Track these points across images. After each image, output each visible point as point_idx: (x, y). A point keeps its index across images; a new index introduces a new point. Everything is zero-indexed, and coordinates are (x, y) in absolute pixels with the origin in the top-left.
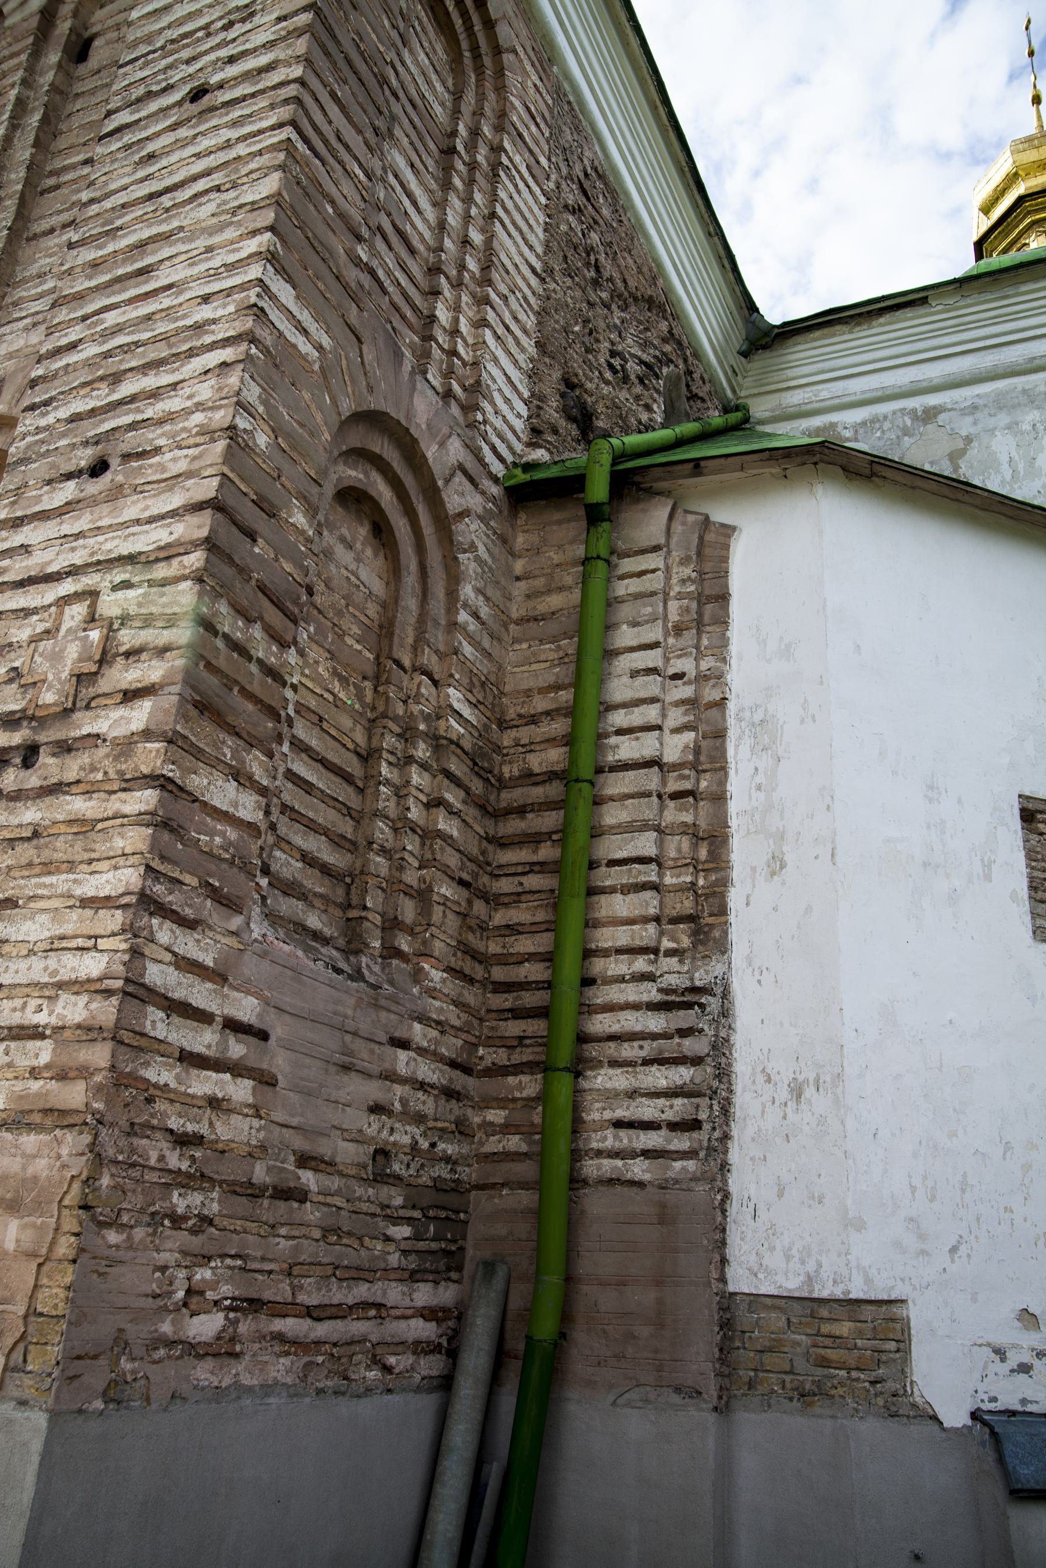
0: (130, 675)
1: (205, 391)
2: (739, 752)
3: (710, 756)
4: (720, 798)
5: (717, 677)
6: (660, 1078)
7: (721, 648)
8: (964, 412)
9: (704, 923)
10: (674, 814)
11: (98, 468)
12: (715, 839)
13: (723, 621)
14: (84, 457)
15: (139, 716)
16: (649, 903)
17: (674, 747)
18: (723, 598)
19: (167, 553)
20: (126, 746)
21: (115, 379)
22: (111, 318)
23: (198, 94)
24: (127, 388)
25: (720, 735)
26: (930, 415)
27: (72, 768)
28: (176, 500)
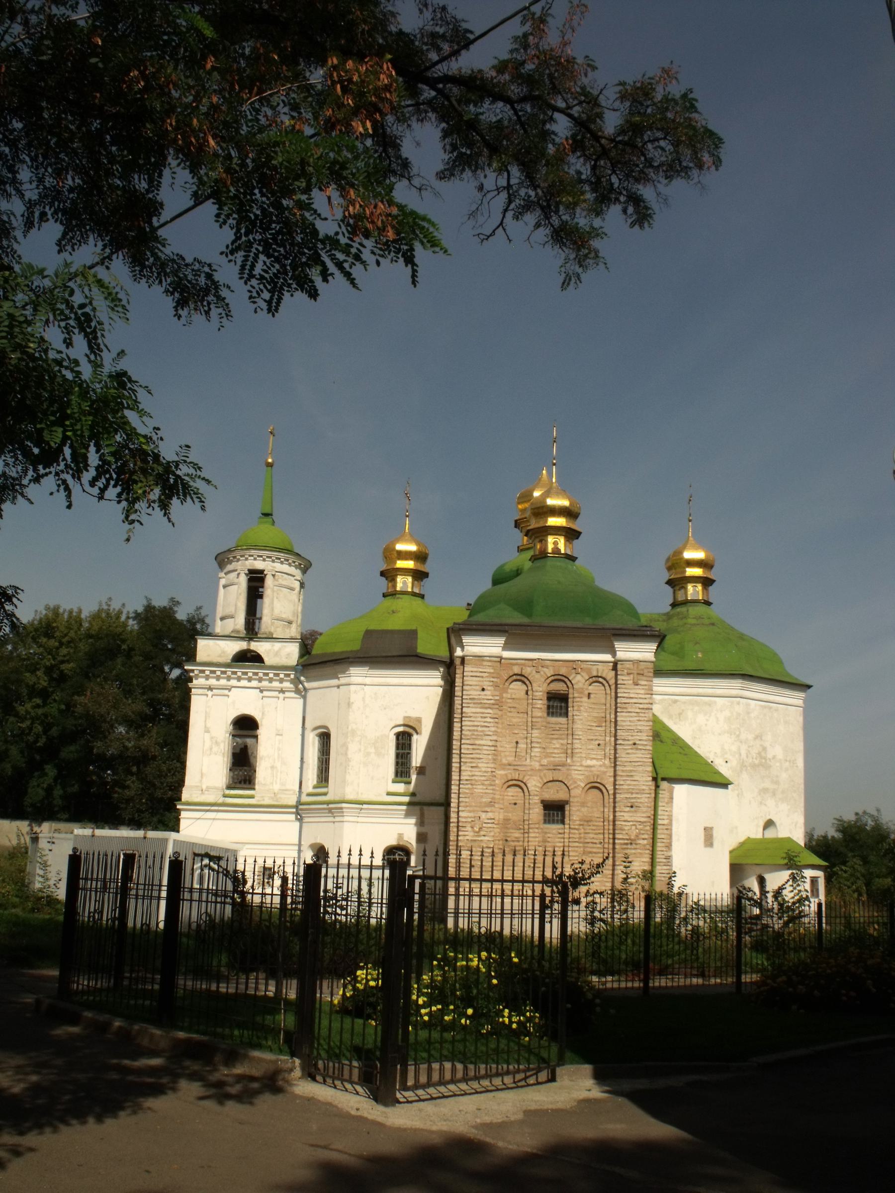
0: (643, 837)
1: (646, 800)
2: (674, 823)
3: (670, 824)
4: (671, 830)
5: (671, 811)
6: (665, 867)
7: (672, 806)
8: (684, 703)
9: (669, 846)
10: (666, 832)
11: (632, 807)
12: (670, 836)
13: (672, 802)
14: (629, 805)
15: (645, 842)
16: (663, 845)
17: (665, 822)
18: (672, 798)
19: (645, 822)
20: (644, 845)
21: (632, 793)
22: (628, 782)
23: (635, 744)
24: (634, 796)
25: (671, 820)
26: (675, 701)
27: (638, 846)
28: (644, 815)
